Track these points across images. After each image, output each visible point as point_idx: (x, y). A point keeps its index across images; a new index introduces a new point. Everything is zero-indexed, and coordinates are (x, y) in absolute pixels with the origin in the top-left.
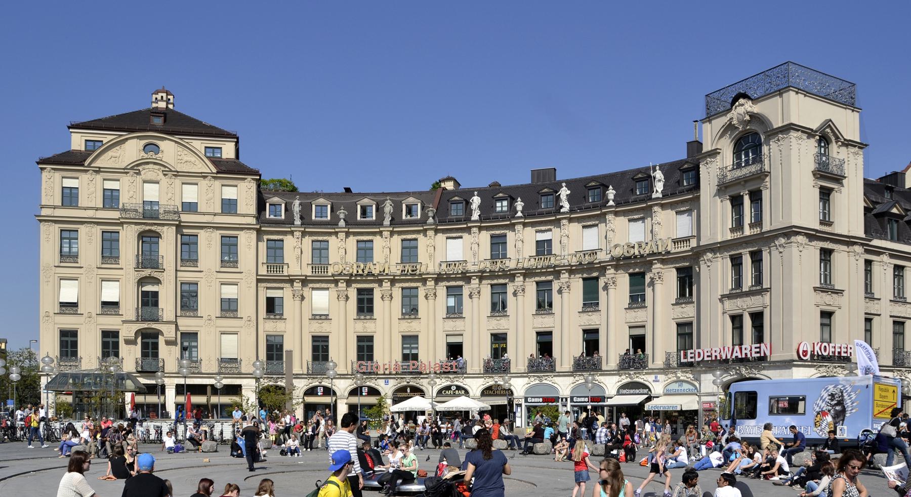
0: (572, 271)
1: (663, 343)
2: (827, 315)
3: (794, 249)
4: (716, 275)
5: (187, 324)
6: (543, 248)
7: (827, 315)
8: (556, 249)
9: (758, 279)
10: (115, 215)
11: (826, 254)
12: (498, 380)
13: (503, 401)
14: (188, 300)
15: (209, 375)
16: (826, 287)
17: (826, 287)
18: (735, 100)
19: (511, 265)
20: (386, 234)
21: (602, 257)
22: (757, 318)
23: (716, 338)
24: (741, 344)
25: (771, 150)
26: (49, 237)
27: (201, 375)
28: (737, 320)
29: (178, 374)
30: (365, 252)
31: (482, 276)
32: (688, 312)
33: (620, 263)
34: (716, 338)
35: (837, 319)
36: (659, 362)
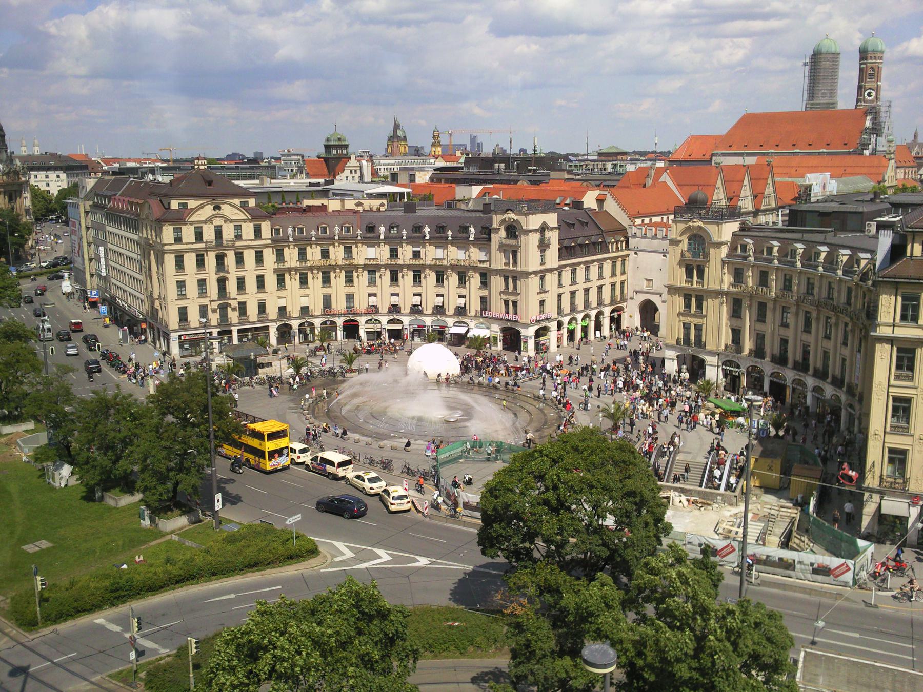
0: (431, 267)
1: (475, 306)
2: (542, 302)
3: (530, 279)
4: (497, 283)
5: (242, 298)
6: (416, 255)
7: (542, 302)
8: (422, 256)
9: (515, 287)
10: (203, 245)
11: (542, 278)
12: (395, 316)
13: (398, 327)
14: (241, 283)
15: (254, 323)
16: (543, 291)
17: (543, 291)
18: (508, 210)
19: (400, 262)
20: (337, 244)
21: (445, 263)
22: (515, 304)
23: (497, 308)
24: (508, 313)
25: (523, 239)
26: (170, 260)
27: (249, 323)
28: (506, 303)
29: (239, 324)
30: (325, 254)
31: (386, 267)
32: (485, 293)
33: (453, 267)
34: (497, 308)
35: (546, 303)
36: (473, 313)
